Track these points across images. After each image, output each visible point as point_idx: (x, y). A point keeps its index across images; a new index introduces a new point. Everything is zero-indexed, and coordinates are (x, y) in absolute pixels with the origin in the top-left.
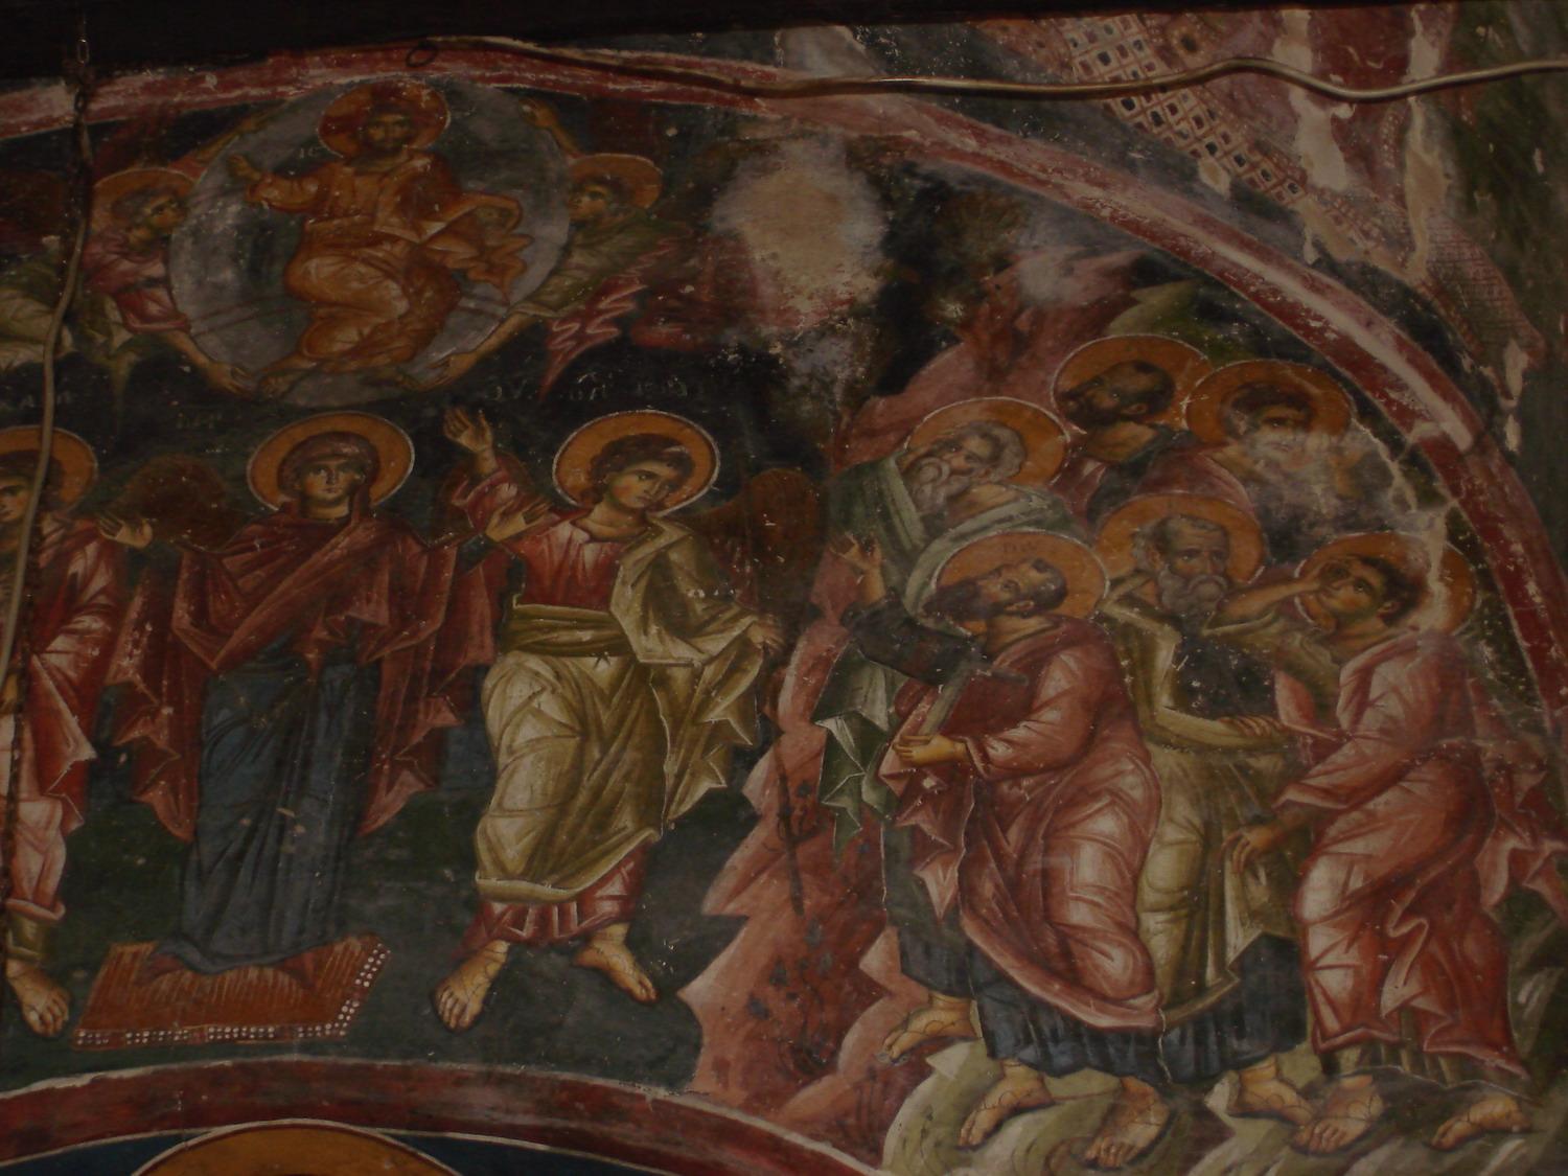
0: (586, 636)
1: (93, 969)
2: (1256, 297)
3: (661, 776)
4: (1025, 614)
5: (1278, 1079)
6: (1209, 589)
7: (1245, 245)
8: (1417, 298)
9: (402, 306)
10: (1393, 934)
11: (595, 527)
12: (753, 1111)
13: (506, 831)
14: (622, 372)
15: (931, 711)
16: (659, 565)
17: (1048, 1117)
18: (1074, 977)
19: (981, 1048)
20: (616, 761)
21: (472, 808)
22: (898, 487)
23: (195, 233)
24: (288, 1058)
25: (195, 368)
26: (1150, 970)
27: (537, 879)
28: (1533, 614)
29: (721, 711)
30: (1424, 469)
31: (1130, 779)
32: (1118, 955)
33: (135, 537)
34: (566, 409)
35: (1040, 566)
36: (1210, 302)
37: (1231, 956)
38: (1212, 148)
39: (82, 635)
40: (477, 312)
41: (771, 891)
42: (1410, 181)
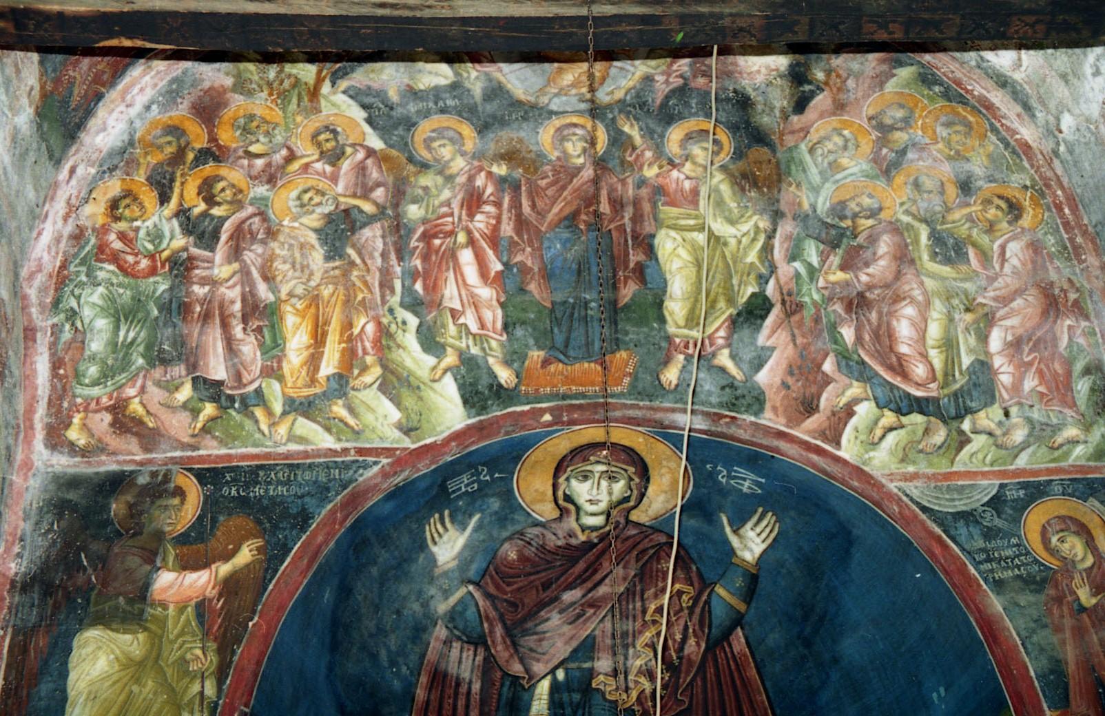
0: (692, 222)
3: (732, 286)
4: (868, 218)
6: (938, 208)
10: (1026, 360)
13: (676, 309)
15: (835, 260)
17: (902, 432)
18: (905, 376)
19: (873, 404)
22: (808, 158)
26: (933, 370)
27: (691, 329)
28: (1068, 223)
29: (752, 257)
33: (501, 170)
34: (668, 116)
35: (870, 196)
37: (964, 367)
41: (782, 337)
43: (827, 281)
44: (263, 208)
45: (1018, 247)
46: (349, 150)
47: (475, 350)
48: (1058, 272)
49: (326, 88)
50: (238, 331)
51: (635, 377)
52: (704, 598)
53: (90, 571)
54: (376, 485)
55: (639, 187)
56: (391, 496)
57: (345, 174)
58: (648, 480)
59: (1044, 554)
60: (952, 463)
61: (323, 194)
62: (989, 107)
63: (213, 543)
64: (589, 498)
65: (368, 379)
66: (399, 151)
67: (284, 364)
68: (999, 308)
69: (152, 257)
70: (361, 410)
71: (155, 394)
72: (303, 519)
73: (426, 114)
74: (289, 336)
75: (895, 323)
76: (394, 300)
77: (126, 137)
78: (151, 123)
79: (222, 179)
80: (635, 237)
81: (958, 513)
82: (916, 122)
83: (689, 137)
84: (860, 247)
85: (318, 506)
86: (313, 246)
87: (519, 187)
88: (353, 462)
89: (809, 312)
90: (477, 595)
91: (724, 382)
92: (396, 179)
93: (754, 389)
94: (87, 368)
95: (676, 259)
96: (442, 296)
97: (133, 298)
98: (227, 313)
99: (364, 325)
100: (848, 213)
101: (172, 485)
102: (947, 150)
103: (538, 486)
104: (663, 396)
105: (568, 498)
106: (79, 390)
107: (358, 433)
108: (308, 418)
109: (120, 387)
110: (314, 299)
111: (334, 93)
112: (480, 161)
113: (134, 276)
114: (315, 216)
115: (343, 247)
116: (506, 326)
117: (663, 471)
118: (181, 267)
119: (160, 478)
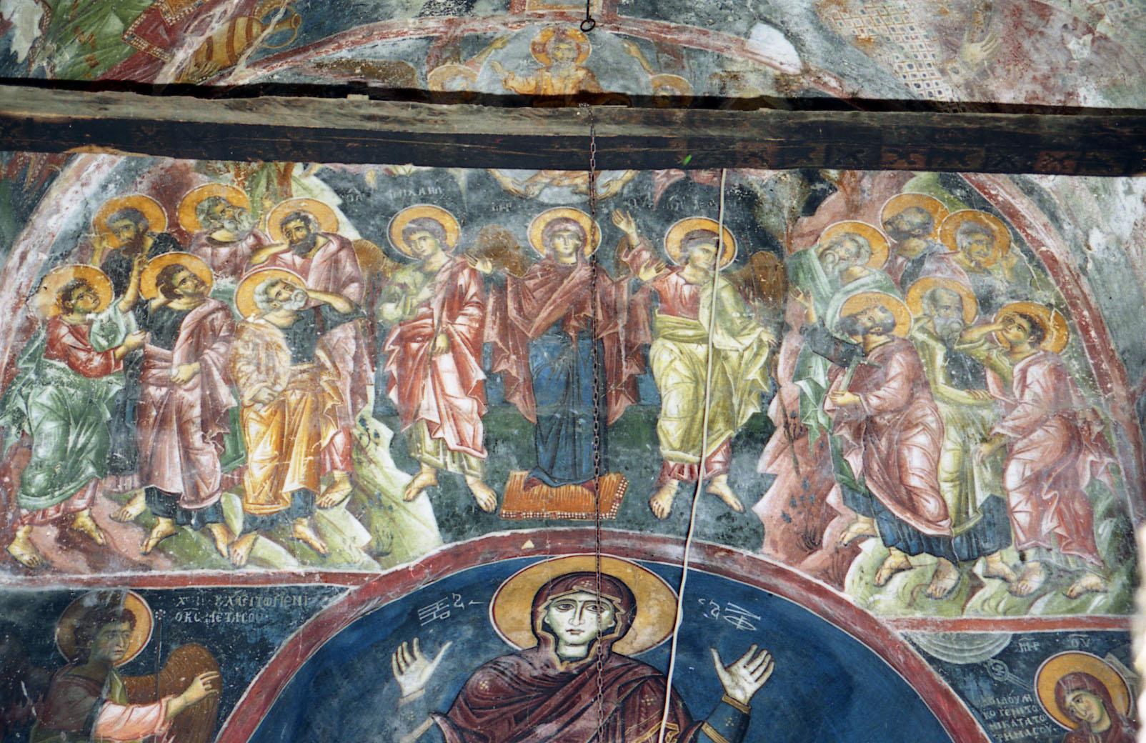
0: (691, 333)
3: (732, 405)
4: (880, 334)
6: (956, 326)
10: (1045, 498)
11: (687, 278)
13: (671, 428)
18: (915, 510)
19: (880, 541)
22: (817, 264)
26: (945, 505)
27: (686, 451)
29: (755, 373)
32: (932, 500)
33: (485, 267)
34: (668, 214)
35: (884, 310)
37: (979, 504)
41: (784, 464)
43: (835, 404)
44: (226, 302)
45: (1041, 372)
46: (321, 240)
47: (453, 468)
48: (1081, 401)
50: (196, 439)
51: (625, 504)
52: (690, 737)
53: (30, 702)
55: (635, 292)
56: (357, 626)
57: (317, 267)
59: (1058, 714)
60: (963, 610)
61: (292, 289)
62: (1014, 214)
63: (164, 674)
65: (336, 496)
66: (375, 243)
67: (246, 478)
69: (105, 354)
70: (328, 531)
71: (106, 507)
72: (263, 650)
73: (406, 203)
74: (251, 446)
75: (906, 452)
76: (367, 410)
77: (80, 220)
78: (108, 204)
80: (629, 347)
81: (968, 665)
82: (935, 229)
83: (689, 238)
84: (871, 366)
85: (279, 636)
86: (279, 346)
87: (506, 287)
88: (318, 588)
89: (814, 438)
90: (444, 727)
91: (720, 512)
92: (372, 274)
93: (752, 520)
94: (34, 476)
95: (672, 374)
96: (419, 406)
97: (84, 399)
98: (185, 419)
99: (334, 437)
100: (859, 328)
101: (121, 608)
102: (967, 262)
104: (654, 525)
105: (547, 628)
106: (24, 500)
107: (324, 556)
108: (270, 538)
109: (68, 498)
110: (280, 406)
111: (307, 176)
112: (463, 257)
113: (86, 375)
114: (282, 313)
115: (312, 347)
116: (487, 443)
117: (651, 603)
118: (136, 366)
119: (108, 600)
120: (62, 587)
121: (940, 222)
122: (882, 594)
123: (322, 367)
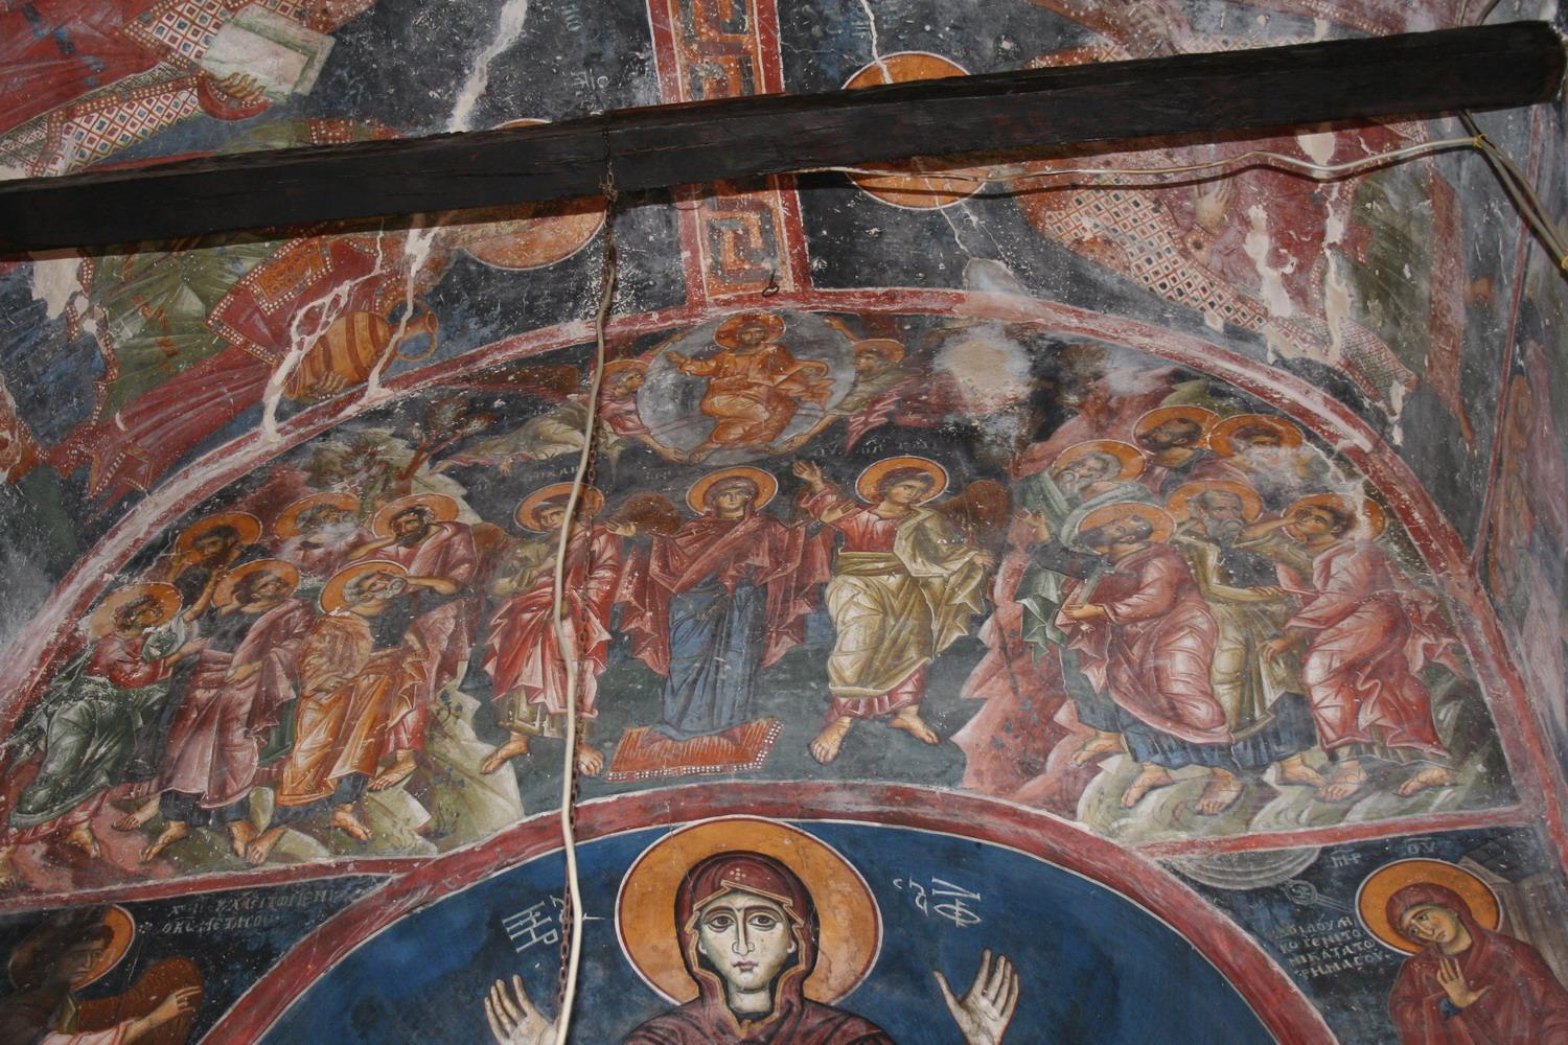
0: (881, 565)
1: (616, 742)
2: (1241, 385)
5: (1305, 764)
7: (1233, 359)
8: (1335, 372)
9: (766, 415)
12: (1000, 796)
13: (845, 662)
14: (889, 439)
15: (1082, 592)
16: (920, 529)
17: (1171, 790)
18: (1178, 719)
19: (1129, 757)
20: (904, 625)
21: (824, 653)
22: (1051, 486)
23: (651, 389)
24: (728, 781)
25: (654, 452)
26: (1223, 714)
28: (1419, 528)
30: (1347, 462)
31: (1200, 620)
34: (861, 457)
35: (1135, 518)
36: (1216, 389)
37: (1268, 704)
38: (1212, 304)
39: (601, 580)
40: (807, 416)
41: (999, 685)
42: (1329, 304)
46: (434, 529)
49: (423, 470)
50: (237, 735)
54: (377, 908)
56: (402, 931)
57: (426, 552)
58: (816, 923)
59: (1392, 937)
60: (1248, 823)
64: (737, 959)
65: (394, 777)
68: (1319, 632)
70: (376, 815)
71: (110, 815)
72: (265, 956)
73: (546, 482)
79: (269, 573)
81: (1255, 891)
87: (650, 547)
97: (117, 710)
100: (1105, 539)
103: (654, 942)
105: (706, 962)
108: (302, 830)
110: (347, 690)
114: (373, 602)
117: (835, 898)
118: (189, 670)
120: (36, 909)
121: (1208, 429)
122: (1133, 816)
123: (410, 650)
